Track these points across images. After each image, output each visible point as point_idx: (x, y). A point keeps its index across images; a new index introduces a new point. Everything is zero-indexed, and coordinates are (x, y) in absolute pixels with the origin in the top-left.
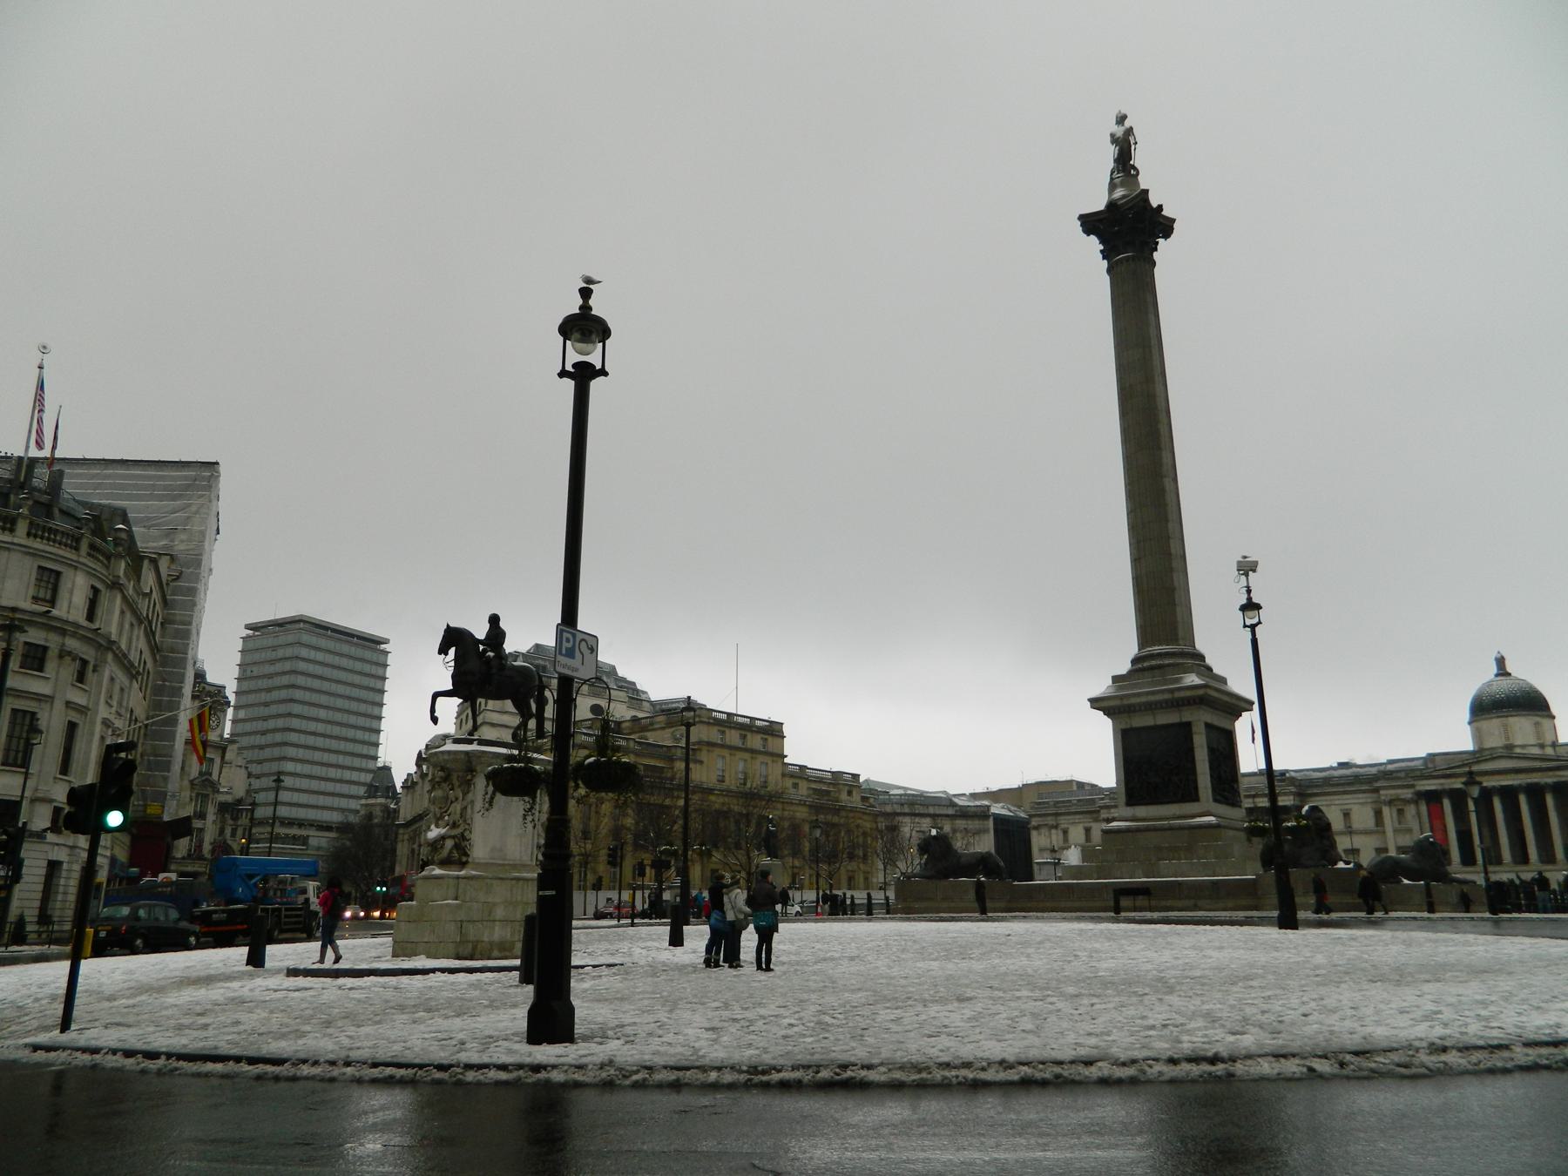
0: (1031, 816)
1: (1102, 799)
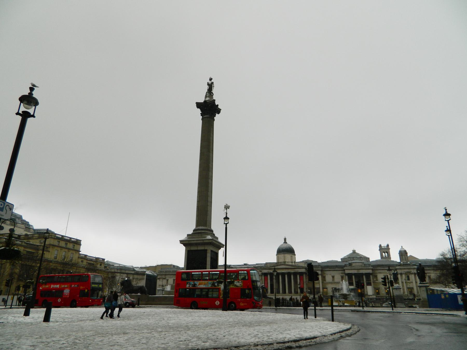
0: (158, 275)
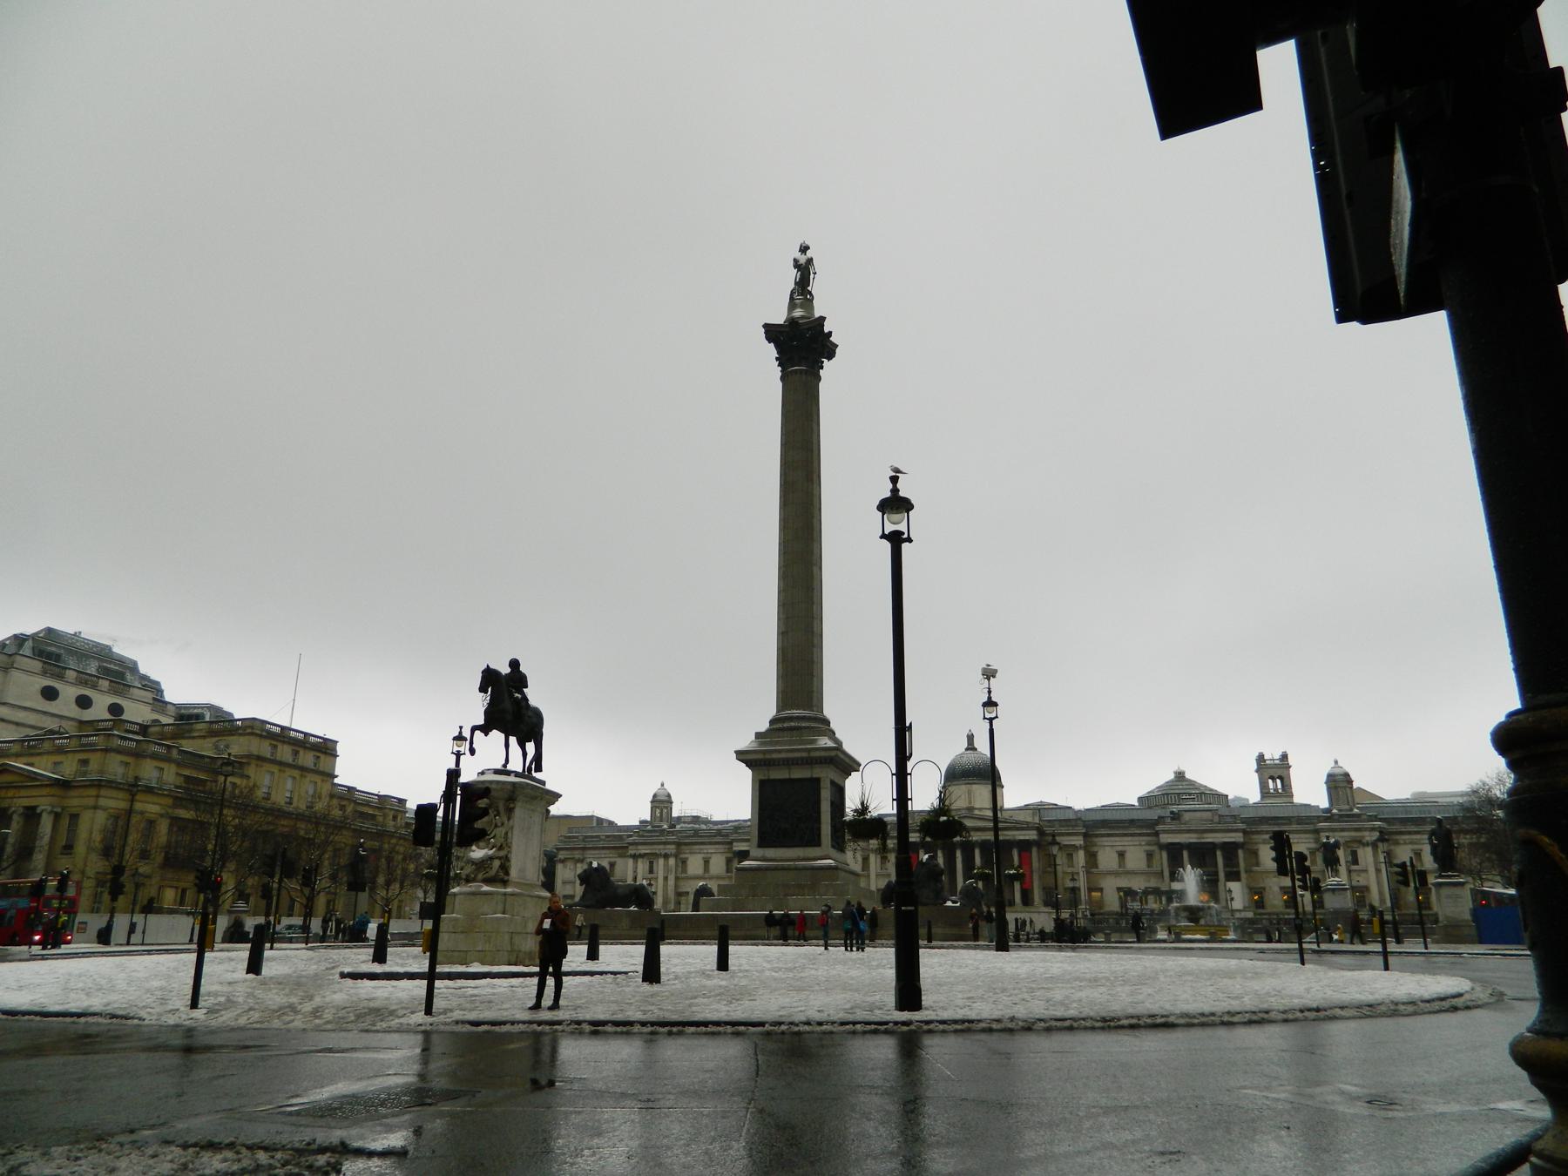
0: (558, 849)
1: (631, 836)
